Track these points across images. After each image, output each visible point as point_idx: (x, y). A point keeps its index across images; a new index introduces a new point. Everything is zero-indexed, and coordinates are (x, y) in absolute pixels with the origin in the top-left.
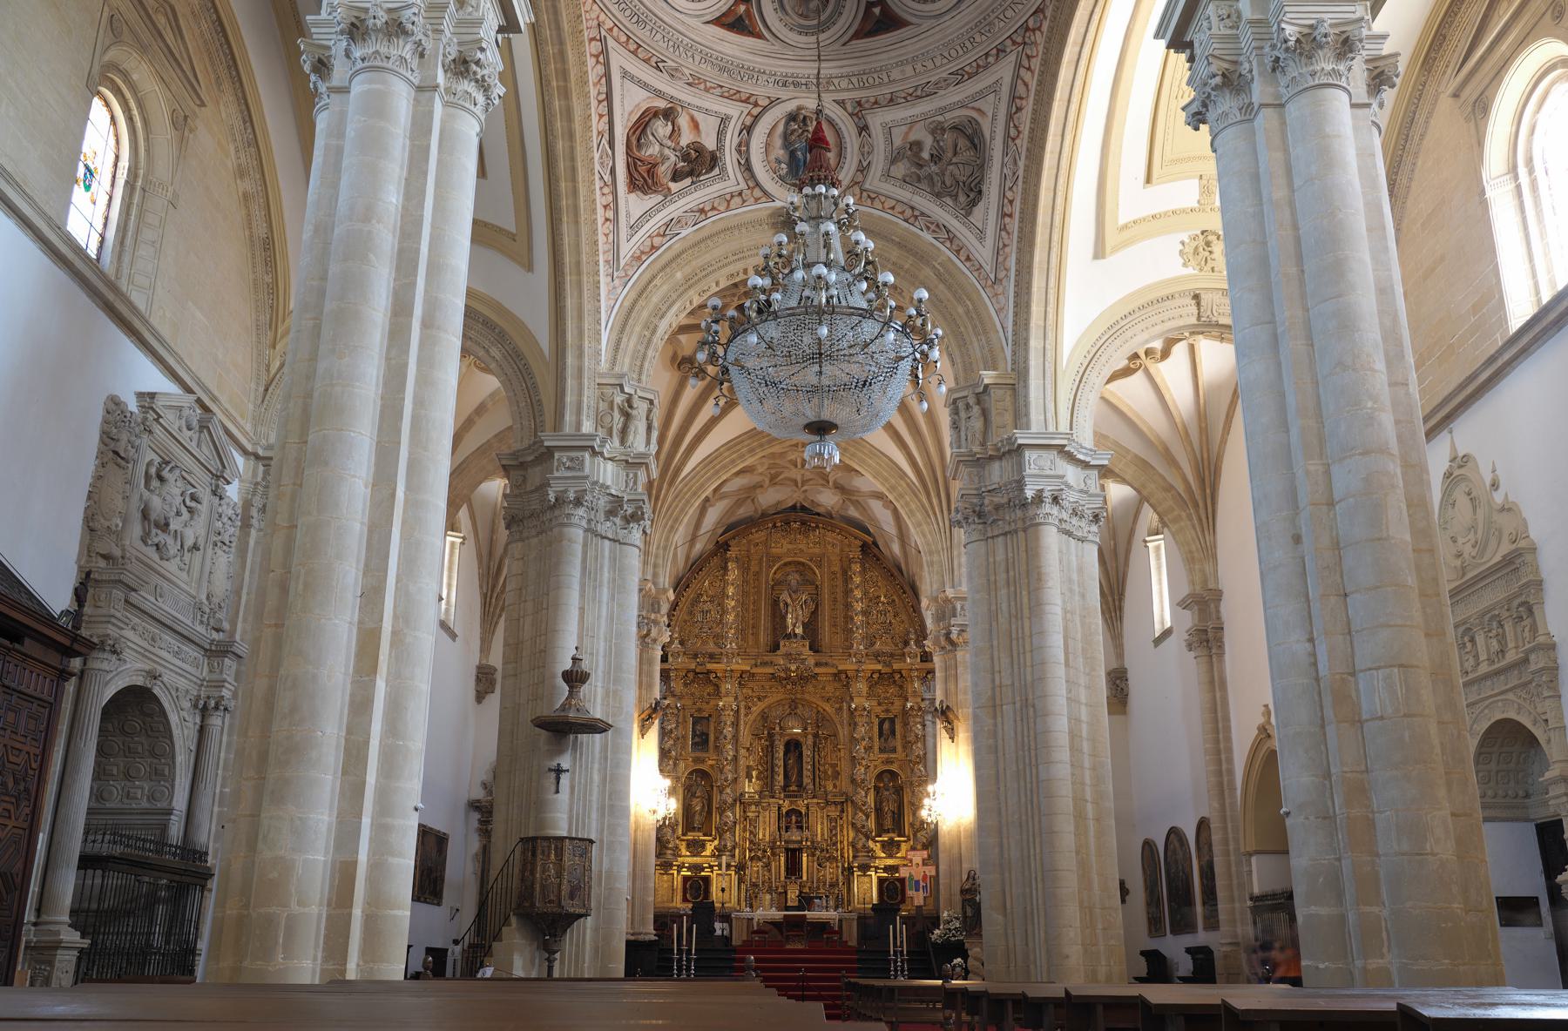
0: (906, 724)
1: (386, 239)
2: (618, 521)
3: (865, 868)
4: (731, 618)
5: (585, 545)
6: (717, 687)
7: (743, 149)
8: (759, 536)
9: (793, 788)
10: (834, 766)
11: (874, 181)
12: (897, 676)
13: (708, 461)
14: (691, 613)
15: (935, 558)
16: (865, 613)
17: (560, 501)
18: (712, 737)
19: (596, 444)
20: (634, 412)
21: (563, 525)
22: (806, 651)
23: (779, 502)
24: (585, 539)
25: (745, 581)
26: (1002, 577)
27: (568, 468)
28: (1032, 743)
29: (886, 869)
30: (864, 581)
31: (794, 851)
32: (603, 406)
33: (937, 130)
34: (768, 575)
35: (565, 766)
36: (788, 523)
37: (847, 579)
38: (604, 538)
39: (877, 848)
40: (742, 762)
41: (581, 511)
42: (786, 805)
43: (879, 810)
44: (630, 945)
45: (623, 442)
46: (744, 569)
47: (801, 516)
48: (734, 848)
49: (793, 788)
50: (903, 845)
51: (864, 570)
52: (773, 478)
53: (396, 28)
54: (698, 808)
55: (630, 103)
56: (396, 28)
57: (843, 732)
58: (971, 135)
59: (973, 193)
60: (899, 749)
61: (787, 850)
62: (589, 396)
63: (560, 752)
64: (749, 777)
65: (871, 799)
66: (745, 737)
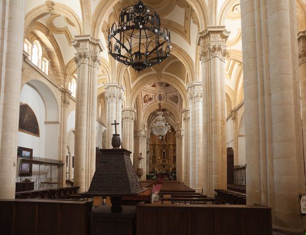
1: (128, 134)
7: (155, 98)
11: (168, 100)
33: (173, 96)
44: (147, 176)
53: (128, 118)
55: (144, 95)
56: (128, 118)
58: (176, 97)
59: (177, 102)
62: (141, 126)
65: (172, 159)
66: (159, 152)
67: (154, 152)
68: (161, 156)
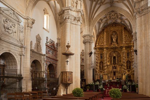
0: (131, 54)
2: (76, 21)
3: (125, 74)
4: (105, 40)
5: (70, 25)
6: (103, 50)
8: (108, 28)
9: (115, 63)
10: (121, 60)
12: (130, 47)
13: (98, 15)
14: (100, 40)
15: (134, 26)
16: (125, 38)
17: (66, 19)
18: (103, 57)
19: (71, 8)
20: (78, 3)
21: (67, 22)
22: (116, 44)
23: (111, 22)
24: (70, 24)
25: (107, 35)
26: (143, 23)
27: (67, 13)
28: (148, 53)
29: (128, 74)
30: (124, 33)
31: (115, 72)
32: (73, 2)
34: (110, 33)
35: (68, 61)
36: (113, 25)
37: (122, 33)
38: (74, 24)
39: (127, 71)
40: (107, 60)
41: (69, 20)
42: (114, 66)
43: (127, 66)
45: (76, 8)
46: (107, 33)
47: (115, 24)
48: (106, 71)
49: (115, 63)
50: (131, 71)
51: (124, 31)
52: (110, 18)
54: (101, 66)
57: (122, 55)
60: (130, 57)
61: (113, 72)
63: (68, 58)
64: (108, 62)
65: (126, 65)
66: (108, 56)
67: (102, 57)
68: (111, 62)
